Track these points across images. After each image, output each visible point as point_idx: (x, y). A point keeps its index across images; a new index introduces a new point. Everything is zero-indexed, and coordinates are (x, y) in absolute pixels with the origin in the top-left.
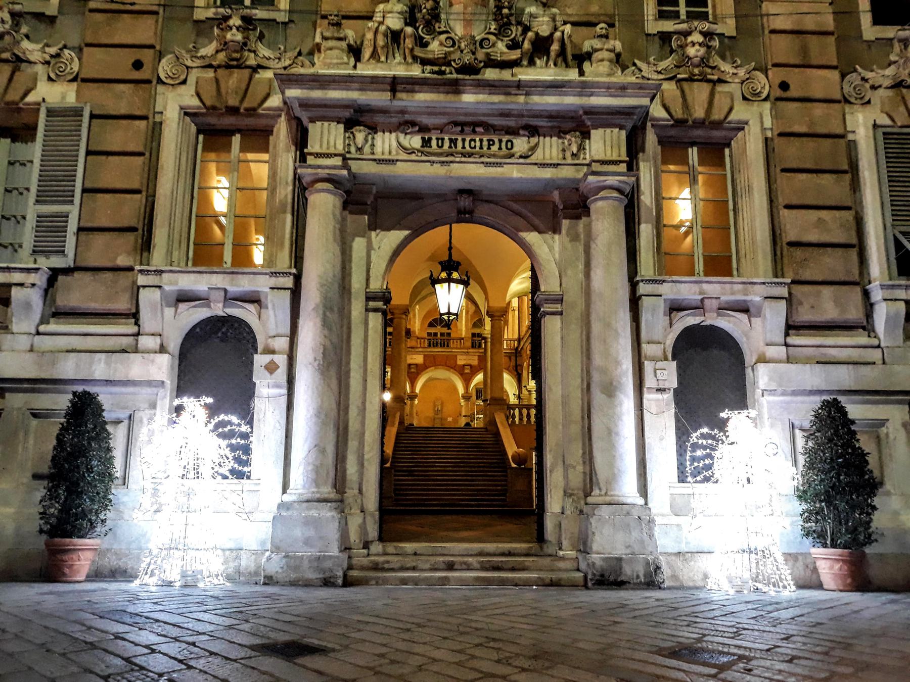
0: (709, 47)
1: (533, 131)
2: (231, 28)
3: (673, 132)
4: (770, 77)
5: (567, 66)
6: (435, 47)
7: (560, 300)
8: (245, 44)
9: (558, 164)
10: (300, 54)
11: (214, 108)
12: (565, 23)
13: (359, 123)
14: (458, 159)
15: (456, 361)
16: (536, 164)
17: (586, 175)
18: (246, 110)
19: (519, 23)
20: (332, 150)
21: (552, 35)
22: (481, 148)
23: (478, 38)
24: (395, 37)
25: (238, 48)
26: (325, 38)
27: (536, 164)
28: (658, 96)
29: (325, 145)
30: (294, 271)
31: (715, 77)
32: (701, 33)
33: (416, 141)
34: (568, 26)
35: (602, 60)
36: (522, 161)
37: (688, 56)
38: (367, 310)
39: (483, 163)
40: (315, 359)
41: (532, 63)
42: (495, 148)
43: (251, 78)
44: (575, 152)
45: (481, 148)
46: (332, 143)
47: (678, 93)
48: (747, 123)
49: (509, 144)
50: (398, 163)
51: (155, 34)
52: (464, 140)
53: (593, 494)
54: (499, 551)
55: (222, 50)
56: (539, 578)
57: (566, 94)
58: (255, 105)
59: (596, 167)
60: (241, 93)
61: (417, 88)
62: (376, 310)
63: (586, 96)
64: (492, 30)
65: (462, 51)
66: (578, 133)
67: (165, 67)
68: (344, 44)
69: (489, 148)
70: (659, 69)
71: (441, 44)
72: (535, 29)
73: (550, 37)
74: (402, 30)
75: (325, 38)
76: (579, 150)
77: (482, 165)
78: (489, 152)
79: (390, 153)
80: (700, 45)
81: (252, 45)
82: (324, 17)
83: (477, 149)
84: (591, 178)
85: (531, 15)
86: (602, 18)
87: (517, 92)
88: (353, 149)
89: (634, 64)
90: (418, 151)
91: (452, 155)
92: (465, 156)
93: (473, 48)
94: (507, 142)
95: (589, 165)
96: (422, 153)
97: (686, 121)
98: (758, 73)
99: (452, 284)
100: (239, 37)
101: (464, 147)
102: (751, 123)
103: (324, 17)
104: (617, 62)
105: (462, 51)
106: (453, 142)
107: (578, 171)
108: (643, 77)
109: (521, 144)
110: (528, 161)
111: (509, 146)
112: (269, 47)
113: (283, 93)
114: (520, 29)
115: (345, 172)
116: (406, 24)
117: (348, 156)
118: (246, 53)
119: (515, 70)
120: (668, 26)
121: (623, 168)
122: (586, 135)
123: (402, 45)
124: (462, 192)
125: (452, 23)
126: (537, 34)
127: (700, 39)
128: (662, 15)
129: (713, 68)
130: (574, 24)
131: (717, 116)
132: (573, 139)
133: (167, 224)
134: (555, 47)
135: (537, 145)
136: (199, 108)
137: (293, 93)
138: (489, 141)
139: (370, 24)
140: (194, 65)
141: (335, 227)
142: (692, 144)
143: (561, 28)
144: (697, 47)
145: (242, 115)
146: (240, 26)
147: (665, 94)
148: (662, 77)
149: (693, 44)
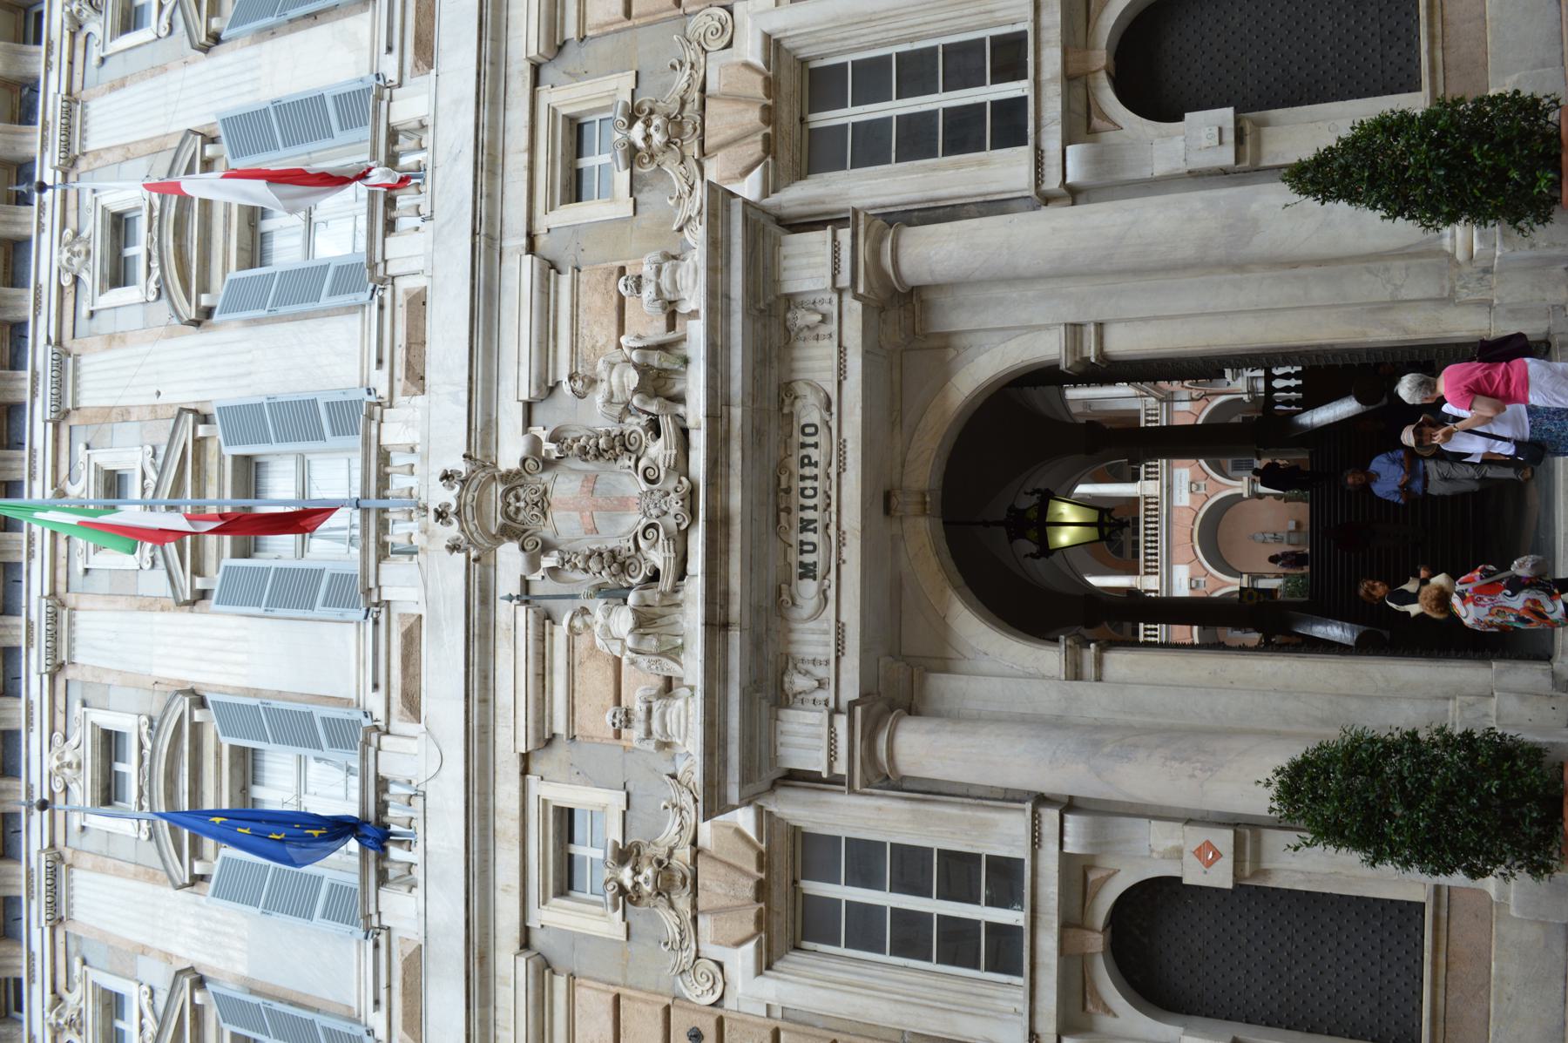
0: (652, 112)
1: (787, 391)
2: (636, 884)
3: (785, 156)
4: (696, 8)
5: (683, 339)
6: (659, 556)
7: (1075, 329)
8: (660, 863)
9: (840, 345)
10: (673, 777)
11: (759, 920)
12: (619, 346)
13: (780, 685)
14: (834, 517)
17: (856, 297)
18: (760, 868)
19: (621, 421)
20: (825, 730)
21: (635, 366)
22: (815, 478)
23: (644, 486)
24: (645, 621)
25: (665, 874)
26: (649, 733)
27: (840, 383)
28: (728, 187)
29: (816, 742)
30: (1028, 806)
31: (697, 95)
32: (630, 126)
33: (808, 590)
34: (623, 340)
35: (674, 283)
36: (834, 409)
37: (668, 143)
38: (1099, 679)
40: (1192, 776)
41: (680, 399)
42: (815, 455)
43: (713, 858)
44: (819, 317)
45: (815, 478)
46: (810, 730)
47: (720, 154)
48: (767, 37)
49: (808, 430)
50: (843, 618)
51: (646, 1002)
52: (803, 508)
53: (1449, 249)
55: (670, 900)
57: (728, 336)
58: (753, 856)
59: (844, 280)
60: (735, 876)
61: (720, 588)
62: (1099, 663)
63: (729, 305)
64: (632, 463)
65: (665, 513)
66: (789, 315)
67: (700, 994)
68: (656, 706)
69: (816, 465)
70: (687, 188)
71: (653, 546)
72: (629, 394)
73: (643, 369)
74: (634, 610)
75: (649, 733)
76: (816, 311)
77: (843, 475)
78: (822, 464)
79: (826, 632)
80: (648, 126)
81: (662, 853)
82: (618, 735)
83: (816, 484)
84: (861, 290)
85: (609, 401)
86: (611, 285)
87: (725, 421)
88: (821, 695)
89: (680, 229)
90: (821, 584)
91: (827, 527)
92: (829, 505)
93: (657, 495)
94: (804, 434)
95: (840, 292)
97: (767, 138)
98: (689, 29)
100: (648, 872)
101: (815, 508)
102: (767, 29)
103: (618, 735)
104: (674, 258)
105: (665, 513)
106: (805, 526)
107: (849, 310)
108: (700, 213)
109: (809, 412)
110: (834, 398)
111: (812, 430)
112: (663, 825)
113: (734, 808)
114: (629, 420)
115: (858, 710)
116: (625, 601)
117: (832, 704)
118: (674, 862)
119: (690, 423)
120: (622, 178)
121: (845, 235)
122: (790, 300)
123: (658, 610)
124: (887, 510)
125: (624, 529)
126: (636, 391)
127: (639, 126)
128: (607, 194)
129: (683, 104)
130: (621, 330)
131: (756, 86)
132: (800, 323)
133: (948, 1016)
134: (655, 359)
135: (809, 383)
136: (758, 945)
137: (734, 794)
138: (803, 465)
139: (625, 661)
140: (693, 946)
141: (952, 732)
142: (802, 120)
143: (627, 351)
144: (652, 130)
145: (768, 876)
146: (633, 869)
147: (726, 174)
148: (698, 182)
149: (647, 138)
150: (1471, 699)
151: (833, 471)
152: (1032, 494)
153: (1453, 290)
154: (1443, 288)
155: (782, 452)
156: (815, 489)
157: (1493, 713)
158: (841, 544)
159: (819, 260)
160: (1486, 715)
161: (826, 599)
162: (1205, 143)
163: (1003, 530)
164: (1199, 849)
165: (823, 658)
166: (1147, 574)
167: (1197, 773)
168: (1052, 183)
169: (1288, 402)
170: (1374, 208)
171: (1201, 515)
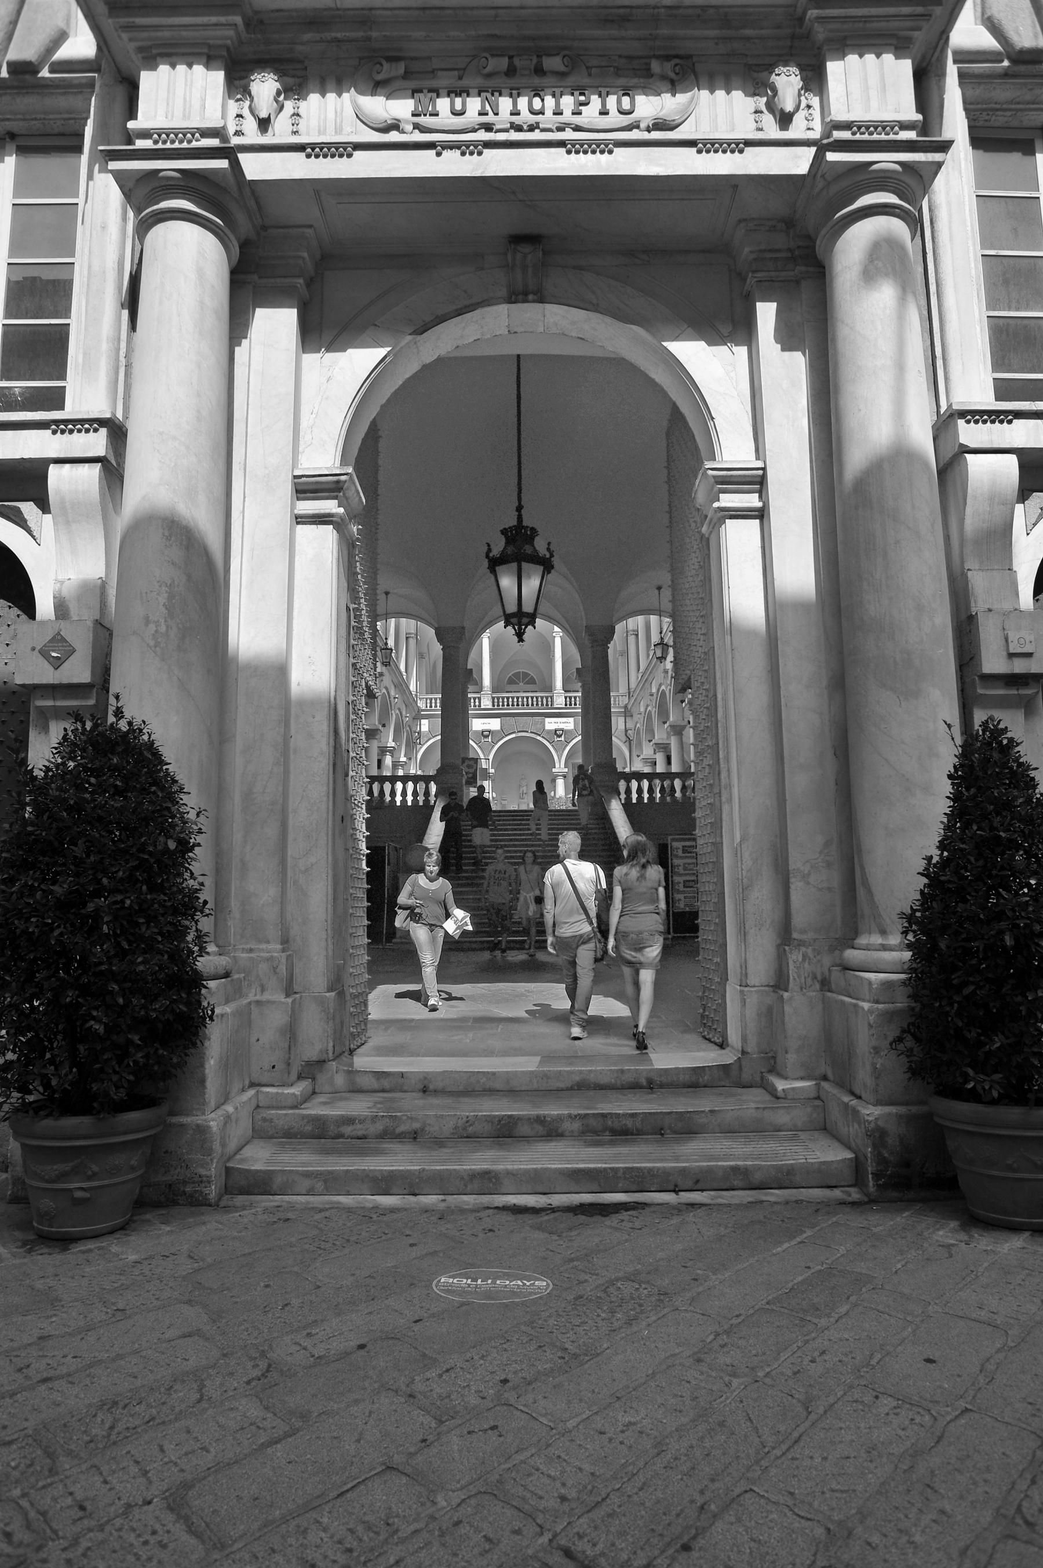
9: (749, 143)
14: (501, 137)
15: (544, 725)
16: (691, 143)
29: (178, 112)
36: (656, 135)
39: (561, 144)
40: (147, 621)
54: (628, 1078)
56: (735, 1169)
78: (577, 120)
83: (549, 113)
96: (417, 126)
99: (524, 565)
107: (797, 157)
124: (518, 239)
150: (283, 969)
151: (568, 135)
152: (548, 549)
153: (801, 943)
154: (804, 931)
155: (594, 62)
156: (541, 112)
157: (266, 996)
158: (465, 148)
159: (874, 103)
160: (263, 989)
161: (386, 129)
162: (1012, 636)
163: (513, 522)
164: (64, 640)
165: (302, 128)
166: (493, 698)
167: (152, 627)
168: (969, 434)
169: (628, 791)
170: (942, 846)
171: (539, 738)
